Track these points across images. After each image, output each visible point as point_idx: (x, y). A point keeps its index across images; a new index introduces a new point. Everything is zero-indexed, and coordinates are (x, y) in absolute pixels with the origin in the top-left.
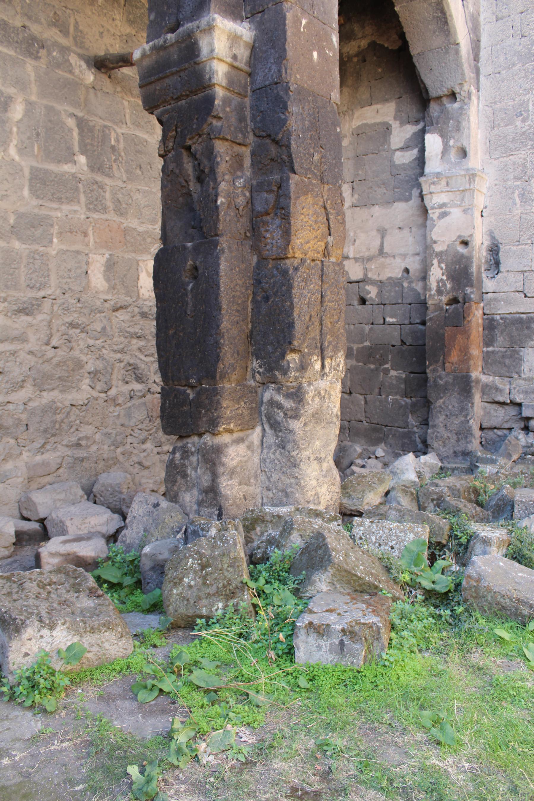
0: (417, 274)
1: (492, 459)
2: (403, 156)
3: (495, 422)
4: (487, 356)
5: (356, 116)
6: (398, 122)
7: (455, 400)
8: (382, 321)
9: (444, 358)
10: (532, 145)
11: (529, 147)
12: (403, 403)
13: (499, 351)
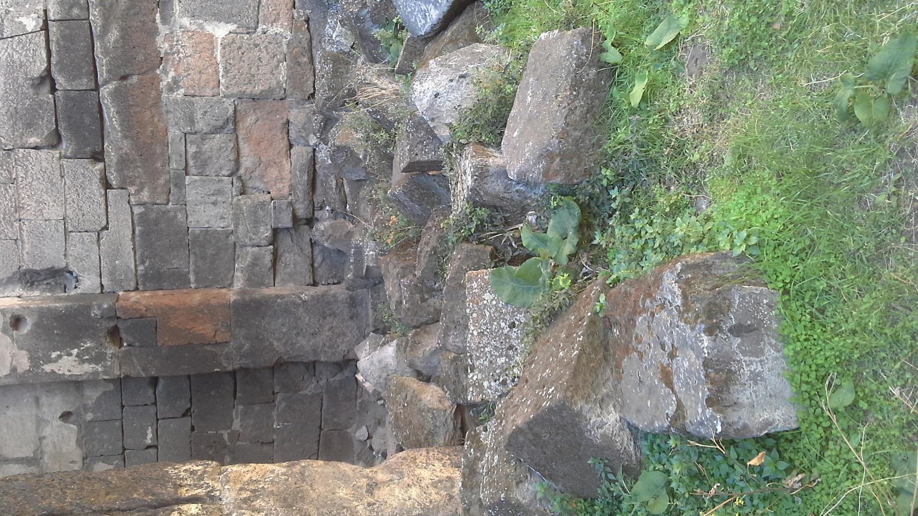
1: (355, 253)
3: (304, 267)
4: (203, 283)
8: (152, 451)
9: (209, 344)
12: (283, 405)
13: (194, 264)
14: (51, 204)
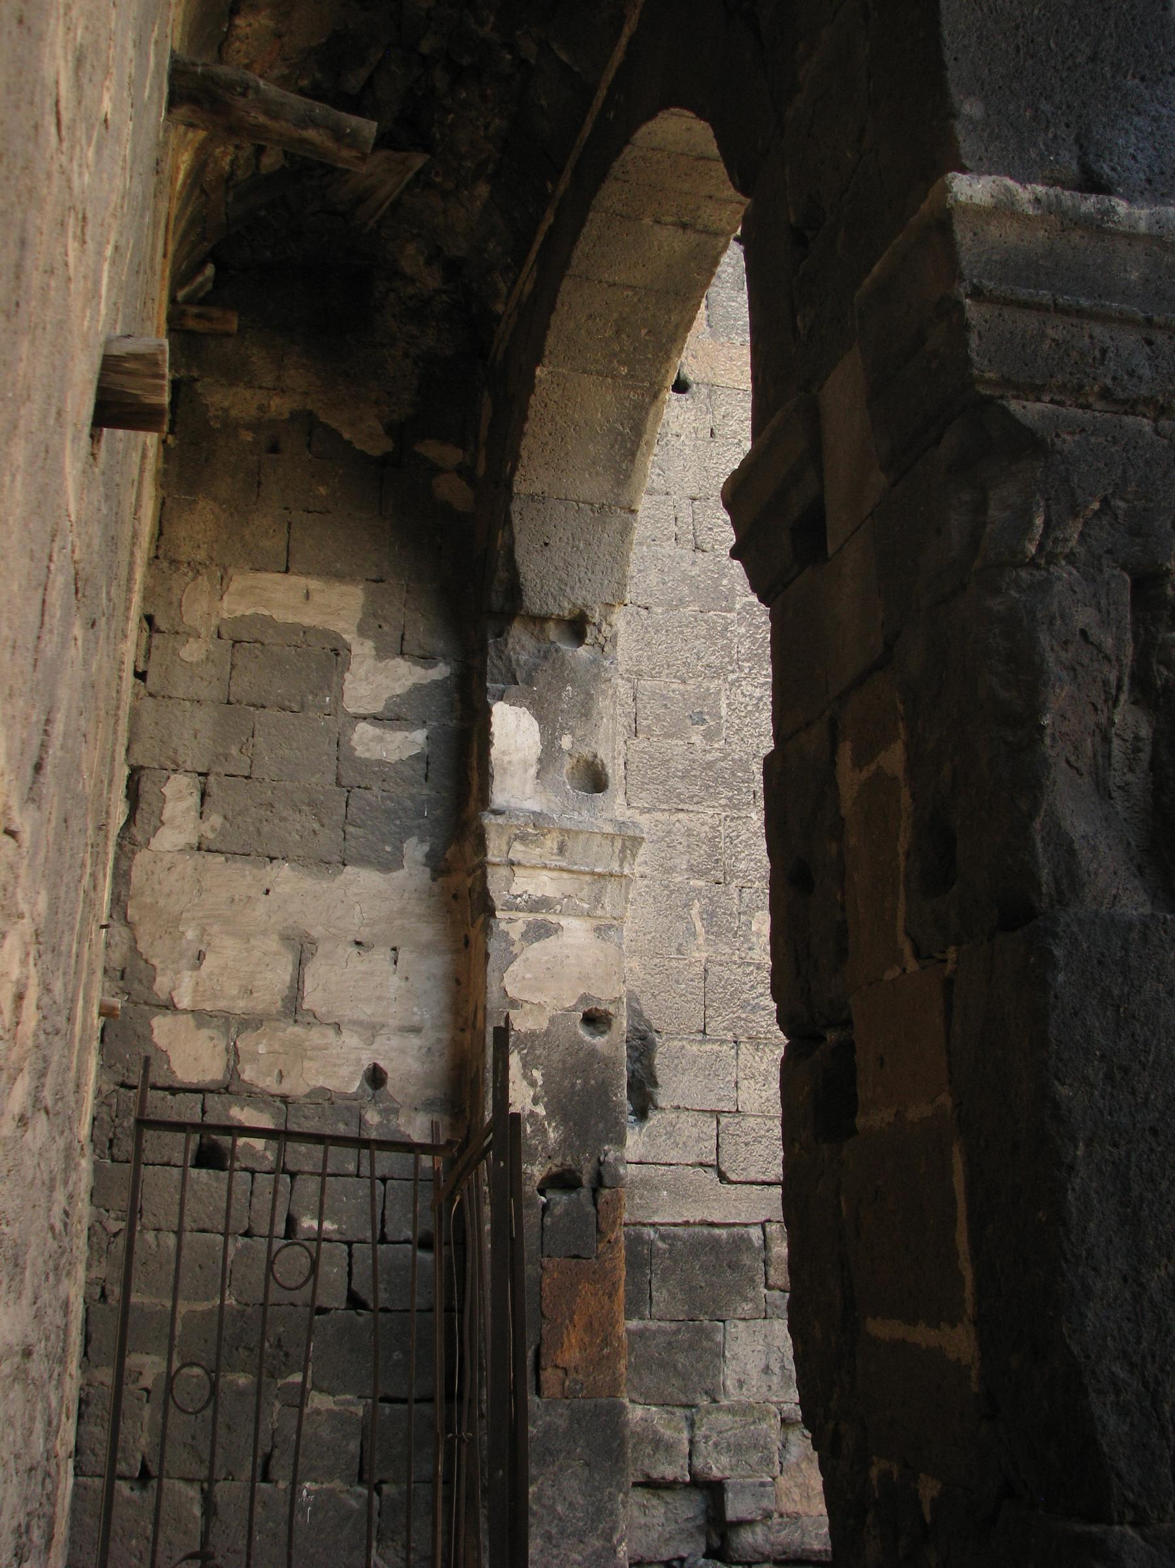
0: (411, 1090)
2: (380, 739)
5: (233, 586)
6: (369, 644)
7: (575, 1484)
10: (730, 799)
11: (723, 802)
13: (660, 1331)
14: (763, 1094)
